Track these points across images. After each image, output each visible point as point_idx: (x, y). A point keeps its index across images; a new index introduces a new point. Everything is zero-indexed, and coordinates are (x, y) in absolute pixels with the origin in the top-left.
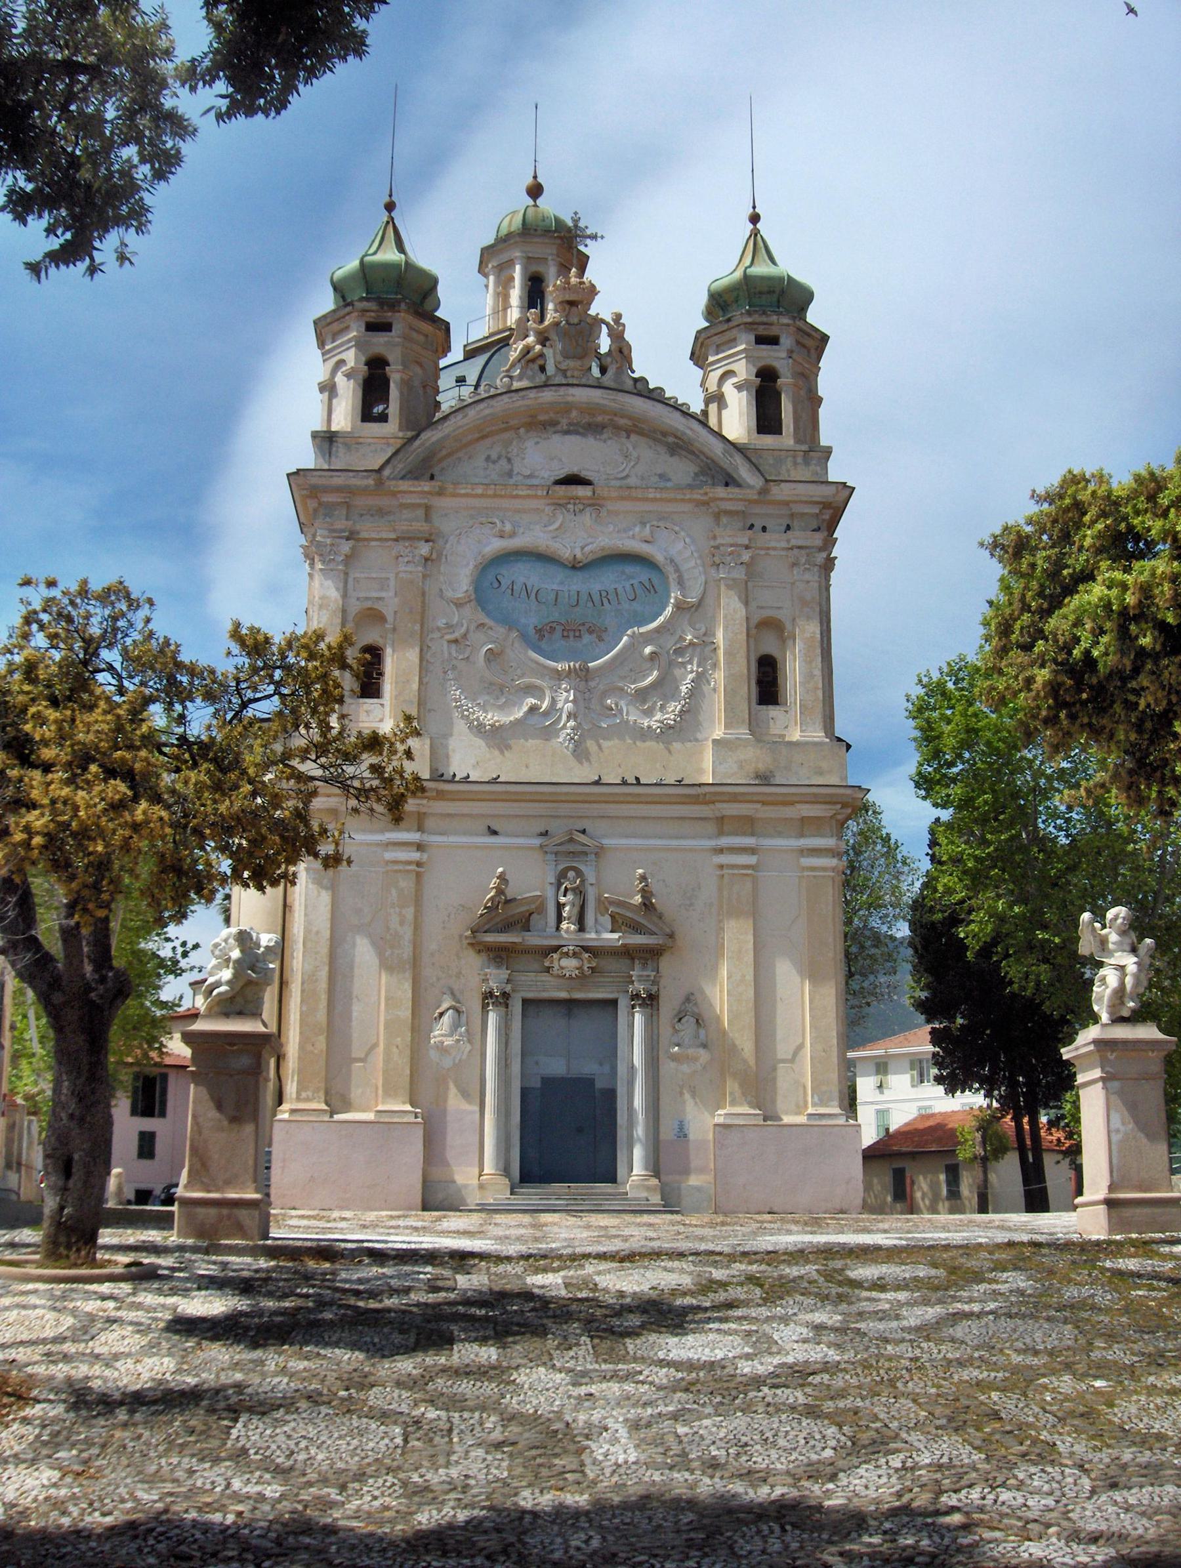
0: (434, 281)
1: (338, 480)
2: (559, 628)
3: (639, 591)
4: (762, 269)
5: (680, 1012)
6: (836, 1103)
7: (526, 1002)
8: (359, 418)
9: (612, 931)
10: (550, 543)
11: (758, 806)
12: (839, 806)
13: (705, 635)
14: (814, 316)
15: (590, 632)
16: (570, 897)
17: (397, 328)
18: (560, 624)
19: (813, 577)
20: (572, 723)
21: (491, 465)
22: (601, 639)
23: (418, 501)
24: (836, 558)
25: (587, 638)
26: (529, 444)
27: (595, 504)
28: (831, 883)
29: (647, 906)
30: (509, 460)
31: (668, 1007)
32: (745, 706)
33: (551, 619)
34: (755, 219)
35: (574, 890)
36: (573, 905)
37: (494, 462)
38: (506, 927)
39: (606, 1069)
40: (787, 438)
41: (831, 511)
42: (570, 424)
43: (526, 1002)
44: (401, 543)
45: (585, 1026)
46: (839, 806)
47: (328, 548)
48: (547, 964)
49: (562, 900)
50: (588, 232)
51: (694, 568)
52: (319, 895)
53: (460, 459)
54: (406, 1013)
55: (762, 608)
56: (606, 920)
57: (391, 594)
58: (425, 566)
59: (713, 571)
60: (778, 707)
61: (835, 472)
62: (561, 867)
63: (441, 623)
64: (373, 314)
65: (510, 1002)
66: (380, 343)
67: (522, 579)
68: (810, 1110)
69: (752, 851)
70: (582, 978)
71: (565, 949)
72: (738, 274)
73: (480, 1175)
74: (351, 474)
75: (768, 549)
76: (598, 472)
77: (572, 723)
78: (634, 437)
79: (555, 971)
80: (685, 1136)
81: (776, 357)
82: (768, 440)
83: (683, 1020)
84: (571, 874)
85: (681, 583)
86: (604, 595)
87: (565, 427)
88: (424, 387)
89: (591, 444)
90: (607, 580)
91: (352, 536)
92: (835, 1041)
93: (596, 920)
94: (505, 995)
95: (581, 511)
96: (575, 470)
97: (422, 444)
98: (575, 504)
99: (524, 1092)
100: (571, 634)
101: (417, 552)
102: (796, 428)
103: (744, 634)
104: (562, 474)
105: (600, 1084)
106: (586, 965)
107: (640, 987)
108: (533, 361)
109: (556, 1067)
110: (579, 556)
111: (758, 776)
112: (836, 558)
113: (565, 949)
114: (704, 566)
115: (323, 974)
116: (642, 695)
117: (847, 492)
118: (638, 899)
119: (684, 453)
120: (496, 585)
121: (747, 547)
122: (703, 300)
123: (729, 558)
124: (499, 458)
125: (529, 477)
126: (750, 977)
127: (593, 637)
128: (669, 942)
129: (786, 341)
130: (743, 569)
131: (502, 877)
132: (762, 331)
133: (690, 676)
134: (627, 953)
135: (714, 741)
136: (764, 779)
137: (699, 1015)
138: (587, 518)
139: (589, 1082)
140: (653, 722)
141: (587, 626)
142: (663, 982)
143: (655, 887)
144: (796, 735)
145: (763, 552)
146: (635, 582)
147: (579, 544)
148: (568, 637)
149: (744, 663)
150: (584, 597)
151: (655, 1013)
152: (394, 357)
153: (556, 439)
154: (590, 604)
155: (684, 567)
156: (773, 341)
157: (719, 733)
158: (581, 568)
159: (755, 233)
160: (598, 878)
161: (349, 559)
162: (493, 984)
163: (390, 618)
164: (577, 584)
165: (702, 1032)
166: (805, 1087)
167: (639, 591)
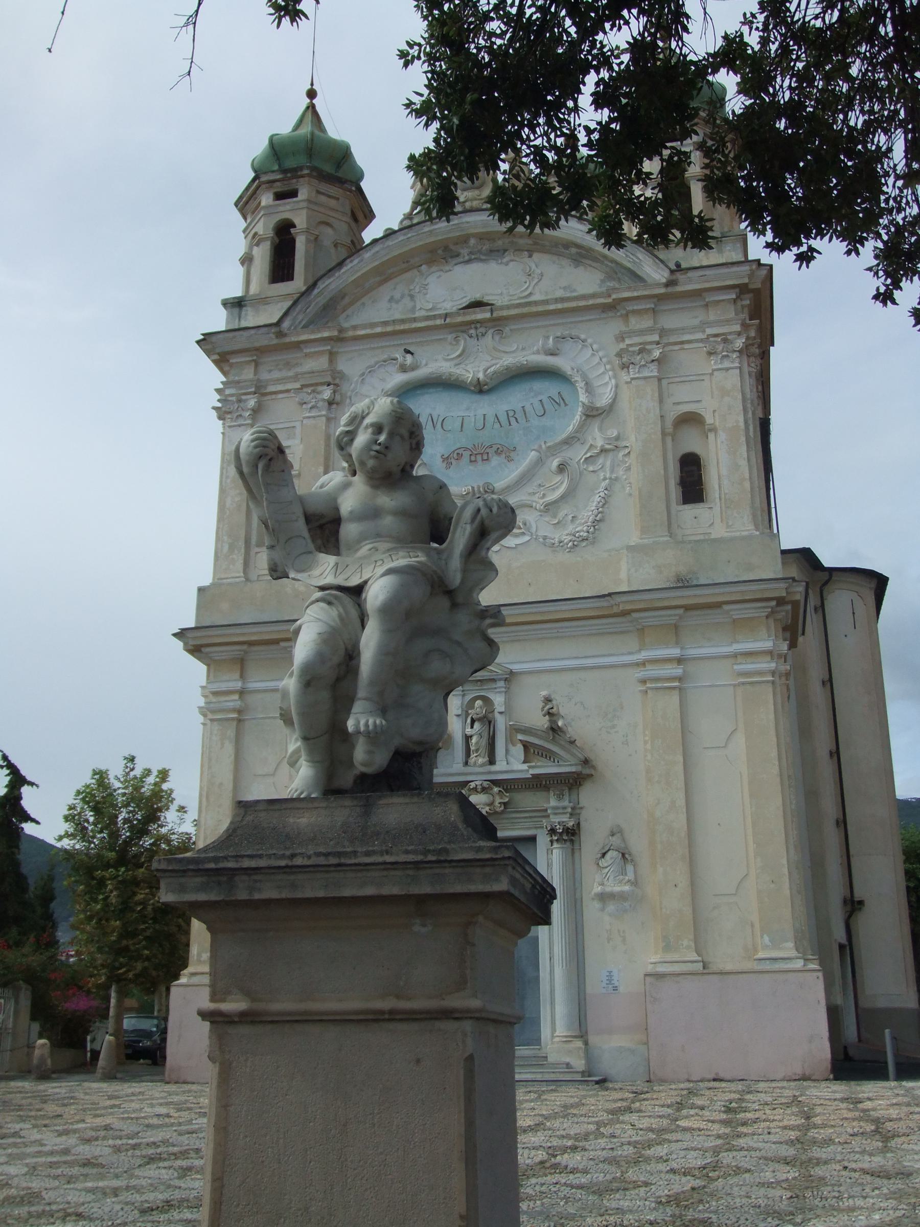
1: (242, 341)
2: (466, 454)
3: (548, 406)
5: (603, 848)
6: (791, 945)
8: (267, 281)
9: (524, 762)
10: (453, 370)
11: (681, 611)
12: (774, 603)
13: (617, 438)
15: (498, 452)
16: (477, 725)
17: (303, 194)
18: (466, 449)
21: (394, 305)
22: (509, 459)
23: (322, 349)
25: (495, 460)
28: (770, 689)
29: (555, 730)
30: (412, 297)
31: (590, 843)
32: (662, 507)
33: (458, 446)
35: (479, 720)
36: (481, 736)
37: (397, 302)
41: (751, 295)
42: (471, 253)
44: (305, 390)
46: (774, 603)
47: (236, 406)
49: (469, 731)
51: (603, 373)
52: (223, 744)
53: (363, 304)
55: (678, 403)
56: (518, 750)
57: (297, 441)
58: (329, 409)
60: (701, 505)
62: (468, 697)
64: (278, 184)
67: (428, 411)
68: (761, 955)
69: (680, 661)
71: (472, 785)
74: (253, 332)
75: (682, 343)
76: (501, 294)
78: (536, 256)
80: (615, 989)
83: (608, 856)
84: (479, 703)
86: (511, 416)
87: (467, 258)
88: (336, 246)
89: (493, 269)
91: (260, 390)
92: (785, 871)
93: (507, 751)
95: (483, 335)
96: (477, 296)
97: (321, 293)
98: (476, 328)
100: (479, 457)
101: (319, 397)
103: (659, 434)
104: (465, 302)
106: (498, 800)
110: (481, 376)
113: (472, 785)
114: (613, 369)
116: (550, 508)
117: (764, 272)
118: (542, 722)
119: (590, 262)
121: (658, 343)
123: (639, 357)
124: (402, 297)
125: (431, 310)
126: (681, 801)
127: (502, 458)
128: (586, 771)
133: (604, 484)
134: (539, 783)
135: (630, 549)
136: (683, 583)
137: (626, 848)
138: (488, 340)
141: (495, 448)
142: (584, 815)
143: (565, 708)
144: (719, 531)
145: (677, 347)
146: (544, 398)
147: (481, 369)
148: (475, 461)
149: (659, 464)
150: (491, 419)
151: (576, 846)
152: (300, 220)
153: (459, 269)
154: (497, 426)
155: (592, 375)
160: (508, 704)
164: (486, 407)
165: (630, 868)
166: (752, 926)
167: (548, 406)
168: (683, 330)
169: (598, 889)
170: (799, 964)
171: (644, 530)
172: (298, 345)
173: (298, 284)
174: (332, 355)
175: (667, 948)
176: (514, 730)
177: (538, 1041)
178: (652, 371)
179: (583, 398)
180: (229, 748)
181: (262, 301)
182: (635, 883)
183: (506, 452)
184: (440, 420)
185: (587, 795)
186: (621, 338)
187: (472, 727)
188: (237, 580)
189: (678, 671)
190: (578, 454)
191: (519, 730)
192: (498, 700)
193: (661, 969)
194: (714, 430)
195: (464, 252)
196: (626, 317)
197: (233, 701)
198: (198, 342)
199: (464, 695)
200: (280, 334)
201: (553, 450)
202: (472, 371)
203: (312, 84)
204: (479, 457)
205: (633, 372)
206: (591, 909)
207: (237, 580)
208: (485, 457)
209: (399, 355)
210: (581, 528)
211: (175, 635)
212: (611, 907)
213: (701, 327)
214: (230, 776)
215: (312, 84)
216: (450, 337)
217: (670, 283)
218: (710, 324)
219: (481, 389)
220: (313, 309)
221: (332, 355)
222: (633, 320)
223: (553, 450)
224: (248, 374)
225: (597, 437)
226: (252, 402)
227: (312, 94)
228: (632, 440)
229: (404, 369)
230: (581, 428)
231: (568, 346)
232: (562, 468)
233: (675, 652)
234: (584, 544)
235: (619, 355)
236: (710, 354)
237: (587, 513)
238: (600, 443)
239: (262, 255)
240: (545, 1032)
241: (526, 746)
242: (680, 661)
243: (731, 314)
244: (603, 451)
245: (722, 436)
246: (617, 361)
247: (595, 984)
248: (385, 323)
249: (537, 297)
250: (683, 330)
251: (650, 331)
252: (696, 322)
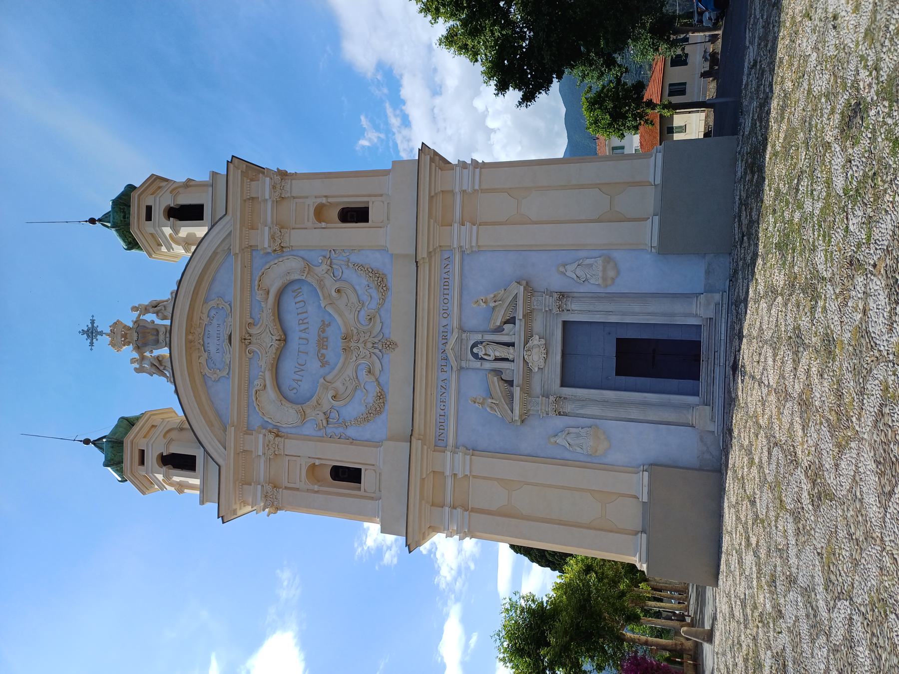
0: (122, 418)
7: (563, 385)
15: (324, 331)
18: (319, 351)
24: (278, 169)
34: (92, 221)
43: (563, 385)
48: (536, 369)
50: (90, 326)
62: (470, 357)
65: (563, 396)
66: (151, 458)
73: (692, 426)
79: (542, 365)
84: (475, 350)
93: (508, 334)
100: (325, 343)
112: (278, 169)
120: (295, 391)
151: (572, 295)
156: (149, 209)
158: (285, 334)
173: (199, 454)
184: (299, 367)
187: (490, 356)
188: (380, 506)
198: (223, 523)
199: (469, 360)
203: (81, 441)
204: (325, 343)
207: (380, 506)
208: (325, 340)
211: (410, 552)
215: (81, 441)
219: (284, 340)
227: (87, 442)
234: (385, 280)
239: (178, 478)
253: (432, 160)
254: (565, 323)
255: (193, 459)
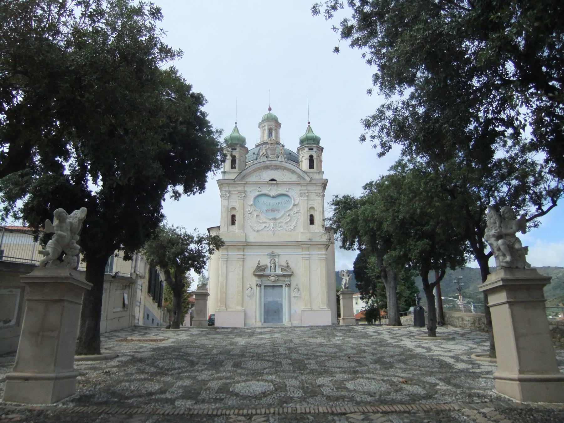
1: (226, 182)
4: (310, 135)
7: (264, 286)
14: (321, 144)
15: (276, 210)
19: (321, 198)
20: (273, 229)
25: (276, 212)
26: (264, 173)
27: (277, 184)
29: (288, 266)
31: (292, 287)
34: (309, 123)
38: (261, 271)
39: (281, 299)
40: (315, 170)
43: (264, 286)
45: (276, 290)
54: (241, 289)
59: (300, 197)
61: (325, 177)
63: (247, 210)
69: (309, 254)
70: (275, 281)
72: (305, 136)
77: (273, 229)
81: (313, 153)
82: (312, 170)
85: (294, 200)
86: (279, 203)
90: (280, 200)
94: (260, 285)
99: (264, 304)
102: (317, 167)
105: (279, 303)
107: (287, 283)
108: (264, 155)
109: (270, 299)
110: (274, 195)
111: (310, 239)
115: (225, 281)
116: (287, 223)
118: (286, 265)
122: (299, 141)
126: (308, 280)
127: (277, 212)
129: (315, 149)
130: (306, 197)
131: (259, 261)
132: (310, 148)
134: (284, 276)
135: (301, 233)
136: (310, 240)
138: (275, 187)
139: (277, 302)
140: (289, 228)
156: (312, 149)
157: (302, 231)
159: (309, 126)
160: (278, 261)
161: (229, 197)
162: (258, 283)
163: (237, 209)
168: (312, 190)
169: (294, 295)
170: (327, 309)
171: (304, 229)
172: (238, 184)
174: (244, 186)
175: (305, 306)
176: (280, 266)
177: (282, 322)
178: (306, 198)
179: (293, 202)
180: (225, 266)
181: (230, 173)
182: (300, 294)
183: (278, 211)
185: (292, 278)
186: (300, 190)
189: (309, 256)
190: (292, 213)
191: (281, 266)
192: (277, 260)
193: (304, 310)
194: (316, 211)
195: (271, 168)
196: (301, 186)
197: (226, 257)
200: (235, 181)
201: (287, 211)
202: (273, 193)
205: (302, 198)
206: (292, 299)
209: (258, 188)
210: (292, 228)
212: (296, 299)
213: (315, 190)
214: (225, 271)
216: (268, 186)
217: (310, 181)
218: (317, 190)
219: (273, 197)
220: (241, 177)
221: (244, 186)
222: (303, 187)
223: (287, 211)
224: (227, 189)
225: (295, 210)
226: (228, 195)
228: (302, 211)
229: (259, 191)
230: (292, 207)
231: (290, 190)
232: (289, 215)
233: (308, 253)
235: (300, 194)
236: (317, 196)
237: (293, 225)
238: (296, 211)
240: (284, 321)
241: (282, 269)
242: (309, 254)
243: (320, 188)
244: (296, 213)
245: (318, 212)
246: (299, 195)
247: (293, 312)
248: (255, 182)
249: (284, 180)
250: (312, 190)
251: (306, 190)
252: (314, 189)
253: (327, 245)
254: (282, 286)
255: (235, 168)
